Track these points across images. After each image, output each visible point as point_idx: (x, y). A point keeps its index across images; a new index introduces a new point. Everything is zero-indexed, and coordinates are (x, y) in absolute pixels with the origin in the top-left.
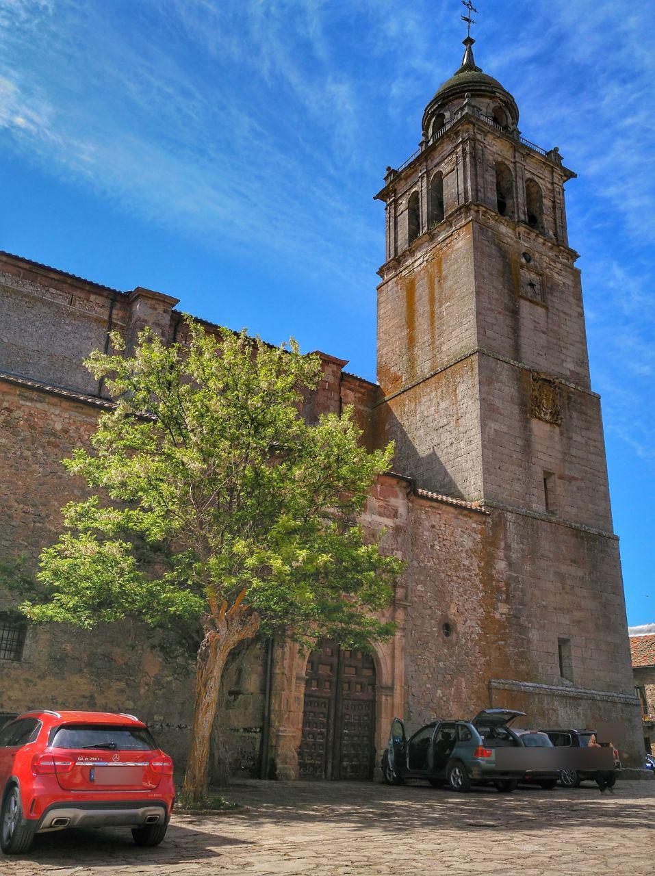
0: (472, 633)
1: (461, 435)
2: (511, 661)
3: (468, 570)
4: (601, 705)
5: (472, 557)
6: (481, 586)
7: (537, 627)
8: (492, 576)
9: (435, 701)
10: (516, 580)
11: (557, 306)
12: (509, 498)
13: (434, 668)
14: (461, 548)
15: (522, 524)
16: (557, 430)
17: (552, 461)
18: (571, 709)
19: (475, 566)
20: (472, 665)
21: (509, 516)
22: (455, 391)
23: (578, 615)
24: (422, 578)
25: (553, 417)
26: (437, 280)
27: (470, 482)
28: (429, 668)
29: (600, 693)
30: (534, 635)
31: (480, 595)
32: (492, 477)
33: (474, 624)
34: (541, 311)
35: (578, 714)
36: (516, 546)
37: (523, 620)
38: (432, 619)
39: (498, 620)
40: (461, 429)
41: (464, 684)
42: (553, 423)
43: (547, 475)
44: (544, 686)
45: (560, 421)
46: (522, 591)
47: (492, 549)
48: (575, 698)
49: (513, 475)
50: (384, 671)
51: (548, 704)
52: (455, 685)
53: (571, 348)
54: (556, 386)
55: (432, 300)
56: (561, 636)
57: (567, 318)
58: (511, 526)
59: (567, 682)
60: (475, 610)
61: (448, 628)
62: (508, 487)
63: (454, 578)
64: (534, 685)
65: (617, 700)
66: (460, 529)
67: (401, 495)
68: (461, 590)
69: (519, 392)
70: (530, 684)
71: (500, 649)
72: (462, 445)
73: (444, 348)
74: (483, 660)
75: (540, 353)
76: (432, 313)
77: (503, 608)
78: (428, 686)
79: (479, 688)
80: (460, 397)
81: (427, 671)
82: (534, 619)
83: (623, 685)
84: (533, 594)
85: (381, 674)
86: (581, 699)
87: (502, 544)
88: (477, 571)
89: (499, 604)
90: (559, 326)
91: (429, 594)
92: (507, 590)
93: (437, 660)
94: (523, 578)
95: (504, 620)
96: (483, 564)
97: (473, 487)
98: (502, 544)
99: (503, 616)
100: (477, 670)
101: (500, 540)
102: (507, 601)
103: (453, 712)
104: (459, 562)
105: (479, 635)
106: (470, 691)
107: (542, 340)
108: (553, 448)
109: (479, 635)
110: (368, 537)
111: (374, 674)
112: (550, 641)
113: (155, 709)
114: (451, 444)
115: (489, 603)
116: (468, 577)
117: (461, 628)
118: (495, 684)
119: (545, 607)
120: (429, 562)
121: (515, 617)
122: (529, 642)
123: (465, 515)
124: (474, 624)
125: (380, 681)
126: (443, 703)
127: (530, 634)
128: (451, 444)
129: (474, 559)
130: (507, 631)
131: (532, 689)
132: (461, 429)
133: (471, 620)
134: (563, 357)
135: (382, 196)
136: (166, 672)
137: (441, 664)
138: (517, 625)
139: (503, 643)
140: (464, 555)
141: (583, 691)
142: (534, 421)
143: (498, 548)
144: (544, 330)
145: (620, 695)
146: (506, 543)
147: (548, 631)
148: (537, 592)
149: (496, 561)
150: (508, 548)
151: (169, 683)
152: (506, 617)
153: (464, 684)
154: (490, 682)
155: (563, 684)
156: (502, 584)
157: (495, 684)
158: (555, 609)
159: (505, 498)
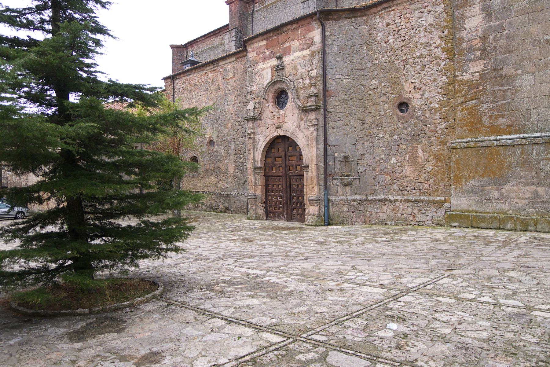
0: (431, 103)
5: (431, 32)
6: (444, 56)
13: (388, 142)
14: (418, 29)
24: (376, 73)
37: (508, 70)
38: (387, 103)
41: (420, 150)
46: (507, 37)
52: (410, 152)
61: (403, 106)
63: (411, 60)
66: (417, 12)
67: (316, 26)
74: (443, 125)
79: (439, 150)
81: (381, 146)
88: (439, 42)
91: (383, 84)
99: (476, 74)
110: (291, 71)
113: (234, 187)
117: (416, 101)
120: (383, 57)
129: (435, 32)
130: (481, 88)
136: (236, 171)
137: (395, 137)
140: (422, 34)
151: (238, 175)
153: (420, 150)
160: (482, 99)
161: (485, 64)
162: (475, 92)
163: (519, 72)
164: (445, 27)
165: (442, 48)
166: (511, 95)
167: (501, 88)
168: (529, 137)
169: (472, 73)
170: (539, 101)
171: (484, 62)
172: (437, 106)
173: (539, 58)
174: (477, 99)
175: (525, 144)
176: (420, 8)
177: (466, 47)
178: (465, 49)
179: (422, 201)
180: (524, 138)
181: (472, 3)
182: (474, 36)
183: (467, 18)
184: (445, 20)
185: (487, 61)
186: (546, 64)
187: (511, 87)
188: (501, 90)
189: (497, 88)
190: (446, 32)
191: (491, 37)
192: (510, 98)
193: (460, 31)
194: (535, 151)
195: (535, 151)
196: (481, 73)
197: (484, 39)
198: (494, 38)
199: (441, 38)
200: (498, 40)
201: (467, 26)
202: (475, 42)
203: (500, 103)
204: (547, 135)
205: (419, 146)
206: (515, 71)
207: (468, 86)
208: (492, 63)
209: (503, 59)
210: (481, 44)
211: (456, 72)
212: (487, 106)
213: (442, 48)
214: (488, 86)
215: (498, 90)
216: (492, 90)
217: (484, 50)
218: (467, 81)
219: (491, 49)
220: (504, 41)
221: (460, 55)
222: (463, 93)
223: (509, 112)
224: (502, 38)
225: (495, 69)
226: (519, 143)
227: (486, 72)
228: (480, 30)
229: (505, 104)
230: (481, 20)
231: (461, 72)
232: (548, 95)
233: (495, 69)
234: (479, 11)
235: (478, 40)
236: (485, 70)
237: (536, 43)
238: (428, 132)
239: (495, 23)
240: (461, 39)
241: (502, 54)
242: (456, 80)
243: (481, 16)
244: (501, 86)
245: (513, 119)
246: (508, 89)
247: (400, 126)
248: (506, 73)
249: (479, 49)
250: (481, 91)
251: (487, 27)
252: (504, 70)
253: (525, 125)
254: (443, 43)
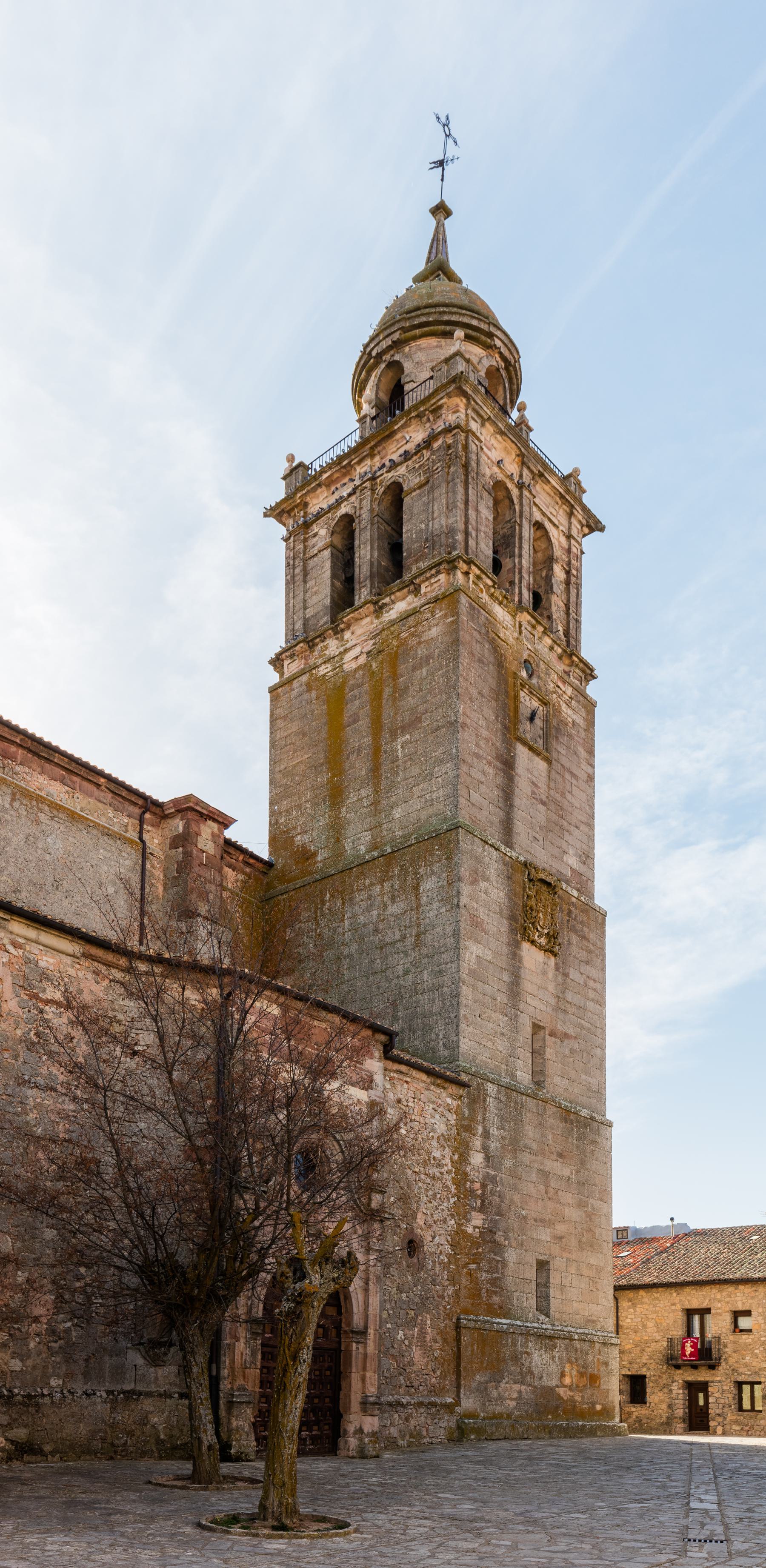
0: (441, 1253)
1: (426, 961)
2: (483, 1291)
3: (439, 1165)
4: (577, 1344)
6: (453, 1188)
7: (514, 1244)
8: (466, 1174)
9: (396, 1346)
10: (494, 1180)
11: (564, 761)
12: (488, 1060)
15: (504, 1099)
16: (552, 961)
17: (543, 1008)
18: (546, 1351)
19: (447, 1161)
20: (439, 1297)
21: (491, 1088)
22: (416, 887)
23: (561, 1228)
25: (549, 942)
26: (388, 691)
27: (437, 1035)
28: (390, 1301)
29: (578, 1331)
30: (511, 1256)
31: (452, 1201)
32: (471, 1029)
33: (443, 1241)
34: (542, 765)
35: (553, 1357)
36: (496, 1133)
37: (499, 1237)
39: (470, 1235)
40: (425, 951)
41: (428, 1322)
42: (550, 951)
43: (537, 1028)
44: (519, 1323)
45: (557, 948)
46: (500, 1196)
47: (467, 1135)
48: (551, 1338)
49: (496, 1028)
50: (355, 1310)
51: (522, 1346)
53: (576, 832)
54: (555, 893)
55: (377, 726)
56: (541, 1258)
57: (574, 782)
58: (491, 1102)
59: (542, 1317)
60: (445, 1221)
62: (489, 1044)
64: (508, 1321)
65: (595, 1339)
68: (430, 1193)
69: (509, 899)
70: (504, 1321)
71: (471, 1275)
72: (426, 975)
73: (397, 813)
75: (537, 836)
76: (376, 751)
77: (477, 1219)
78: (389, 1326)
79: (445, 1327)
80: (424, 899)
82: (511, 1235)
83: (601, 1320)
84: (512, 1200)
85: (350, 1312)
86: (558, 1338)
87: (480, 1129)
88: (450, 1167)
89: (473, 1213)
90: (563, 794)
92: (483, 1193)
93: (400, 1290)
94: (501, 1178)
95: (478, 1235)
96: (456, 1157)
97: (441, 1043)
98: (480, 1129)
99: (477, 1230)
100: (444, 1303)
101: (478, 1122)
102: (481, 1210)
103: (416, 1360)
104: (429, 1154)
105: (448, 1256)
106: (435, 1332)
107: (541, 814)
108: (546, 989)
109: (448, 1256)
111: (339, 1313)
112: (527, 1263)
114: (406, 973)
115: (461, 1214)
116: (438, 1174)
117: (429, 1247)
118: (465, 1322)
119: (524, 1218)
121: (491, 1231)
122: (505, 1265)
123: (438, 1086)
124: (443, 1241)
125: (349, 1323)
126: (404, 1348)
127: (506, 1255)
128: (406, 973)
130: (480, 1250)
131: (505, 1327)
132: (425, 951)
133: (440, 1235)
134: (564, 846)
135: (278, 512)
137: (404, 1296)
138: (491, 1242)
139: (474, 1266)
141: (559, 1328)
142: (526, 945)
143: (474, 1135)
144: (544, 799)
145: (599, 1333)
146: (484, 1128)
147: (526, 1251)
148: (517, 1198)
149: (471, 1153)
150: (486, 1134)
152: (480, 1232)
153: (428, 1322)
154: (458, 1319)
155: (538, 1319)
156: (477, 1186)
157: (465, 1322)
158: (535, 1220)
159: (484, 1062)
172: (446, 1260)
179: (433, 1404)
189: (492, 1256)
198: (491, 1191)
205: (428, 1316)
230: (481, 1160)
238: (436, 1298)
247: (409, 1278)
250: (480, 1254)
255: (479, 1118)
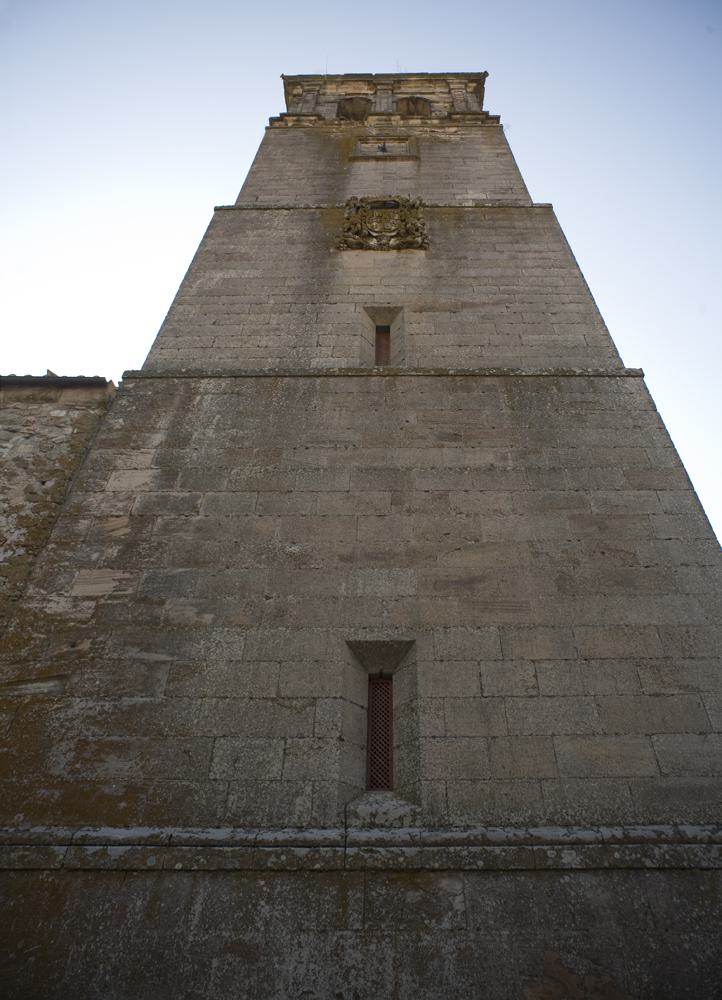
37: (179, 609)
87: (158, 438)
88: (20, 500)
99: (87, 604)
130: (85, 645)
160: (76, 679)
161: (120, 580)
162: (61, 656)
163: (208, 618)
164: (53, 473)
165: (20, 518)
166: (168, 682)
167: (145, 655)
168: (189, 843)
169: (75, 599)
170: (246, 713)
171: (119, 574)
173: (266, 592)
174: (60, 677)
175: (172, 871)
176: (12, 422)
177: (88, 529)
178: (84, 533)
180: (170, 844)
181: (140, 443)
182: (118, 510)
183: (115, 469)
184: (61, 460)
185: (127, 575)
186: (281, 613)
187: (176, 658)
188: (142, 661)
189: (134, 652)
190: (49, 484)
191: (159, 520)
192: (162, 689)
193: (87, 491)
194: (198, 908)
195: (198, 908)
196: (102, 601)
197: (141, 520)
199: (30, 493)
200: (173, 531)
201: (111, 484)
202: (113, 523)
203: (127, 701)
204: (251, 837)
206: (198, 614)
207: (48, 632)
208: (142, 581)
209: (173, 576)
210: (128, 530)
211: (31, 587)
212: (83, 704)
213: (20, 518)
214: (110, 643)
215: (135, 660)
216: (115, 656)
217: (129, 546)
218: (50, 619)
219: (150, 549)
220: (189, 537)
221: (61, 544)
222: (24, 653)
223: (146, 739)
224: (185, 527)
225: (144, 600)
226: (151, 862)
227: (115, 602)
228: (138, 499)
229: (142, 708)
230: (148, 480)
231: (45, 589)
232: (273, 700)
233: (144, 600)
234: (150, 461)
235: (126, 520)
236: (116, 598)
237: (263, 557)
239: (177, 494)
240: (81, 511)
241: (173, 564)
242: (21, 609)
243: (150, 472)
244: (148, 649)
245: (154, 762)
246: (164, 662)
248: (172, 614)
249: (117, 541)
250: (81, 655)
251: (157, 497)
252: (167, 606)
253: (189, 791)
254: (30, 505)
255: (163, 423)
